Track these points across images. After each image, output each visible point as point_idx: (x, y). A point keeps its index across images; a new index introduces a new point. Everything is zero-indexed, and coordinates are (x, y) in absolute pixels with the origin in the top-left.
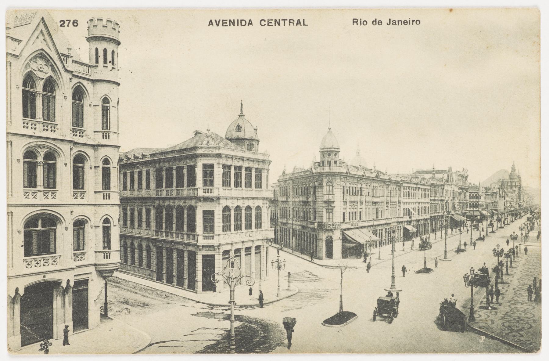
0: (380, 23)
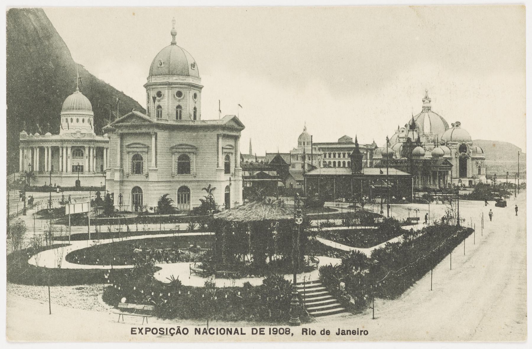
0: (328, 333)
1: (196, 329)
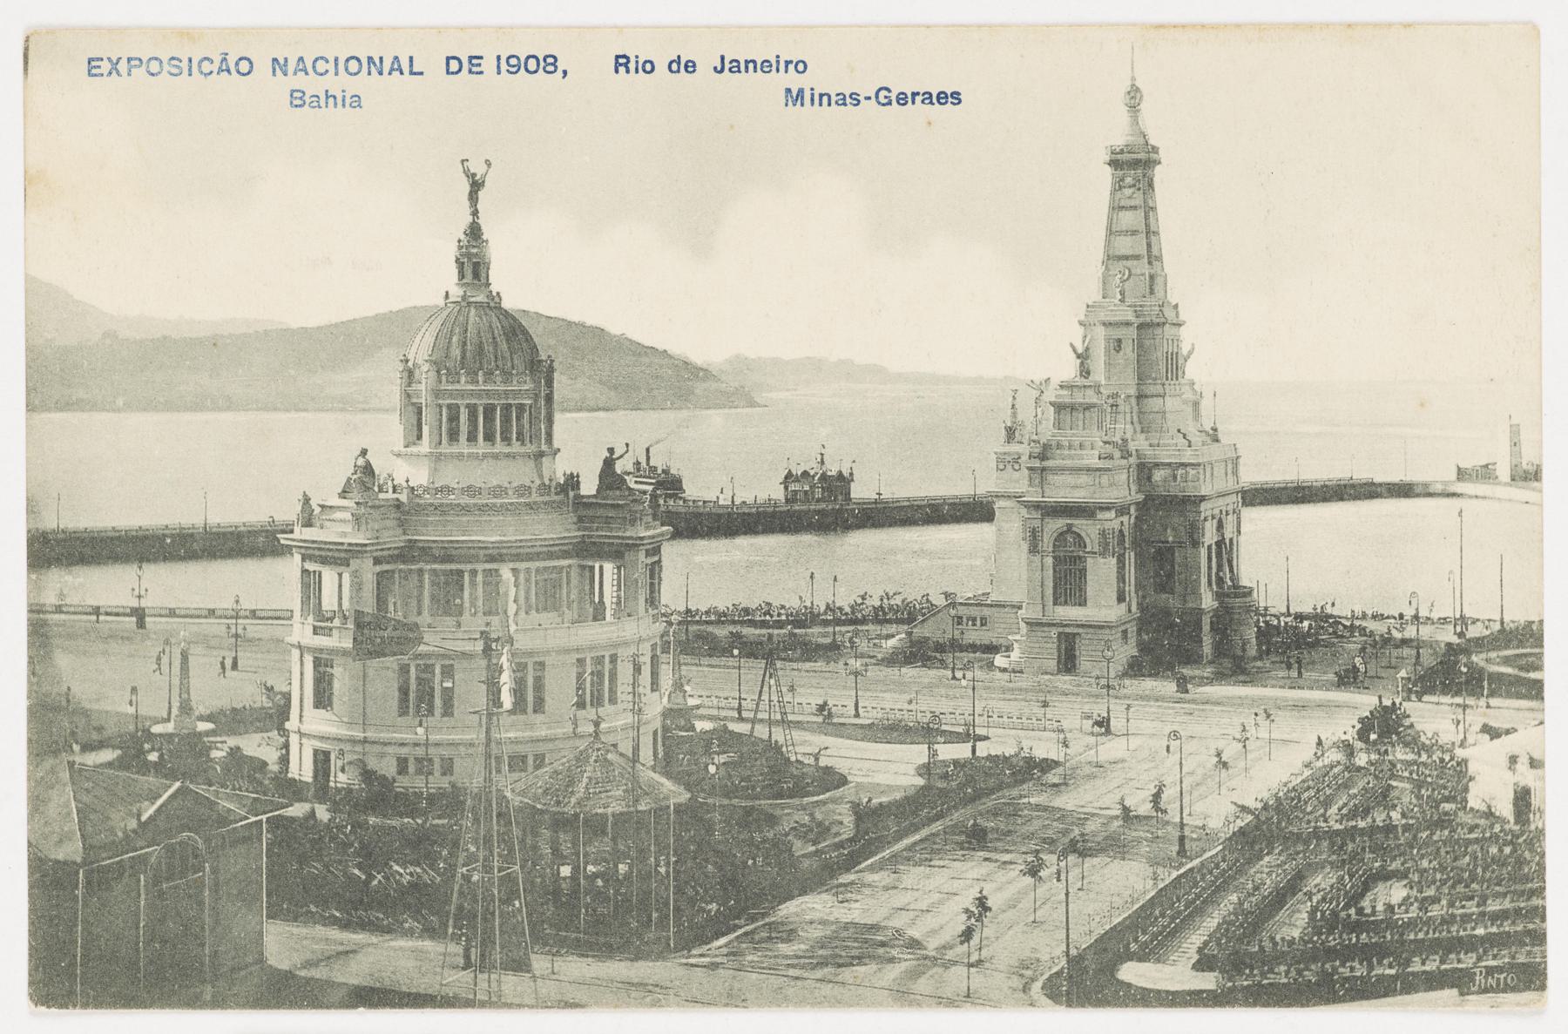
0: (690, 67)
1: (275, 60)
